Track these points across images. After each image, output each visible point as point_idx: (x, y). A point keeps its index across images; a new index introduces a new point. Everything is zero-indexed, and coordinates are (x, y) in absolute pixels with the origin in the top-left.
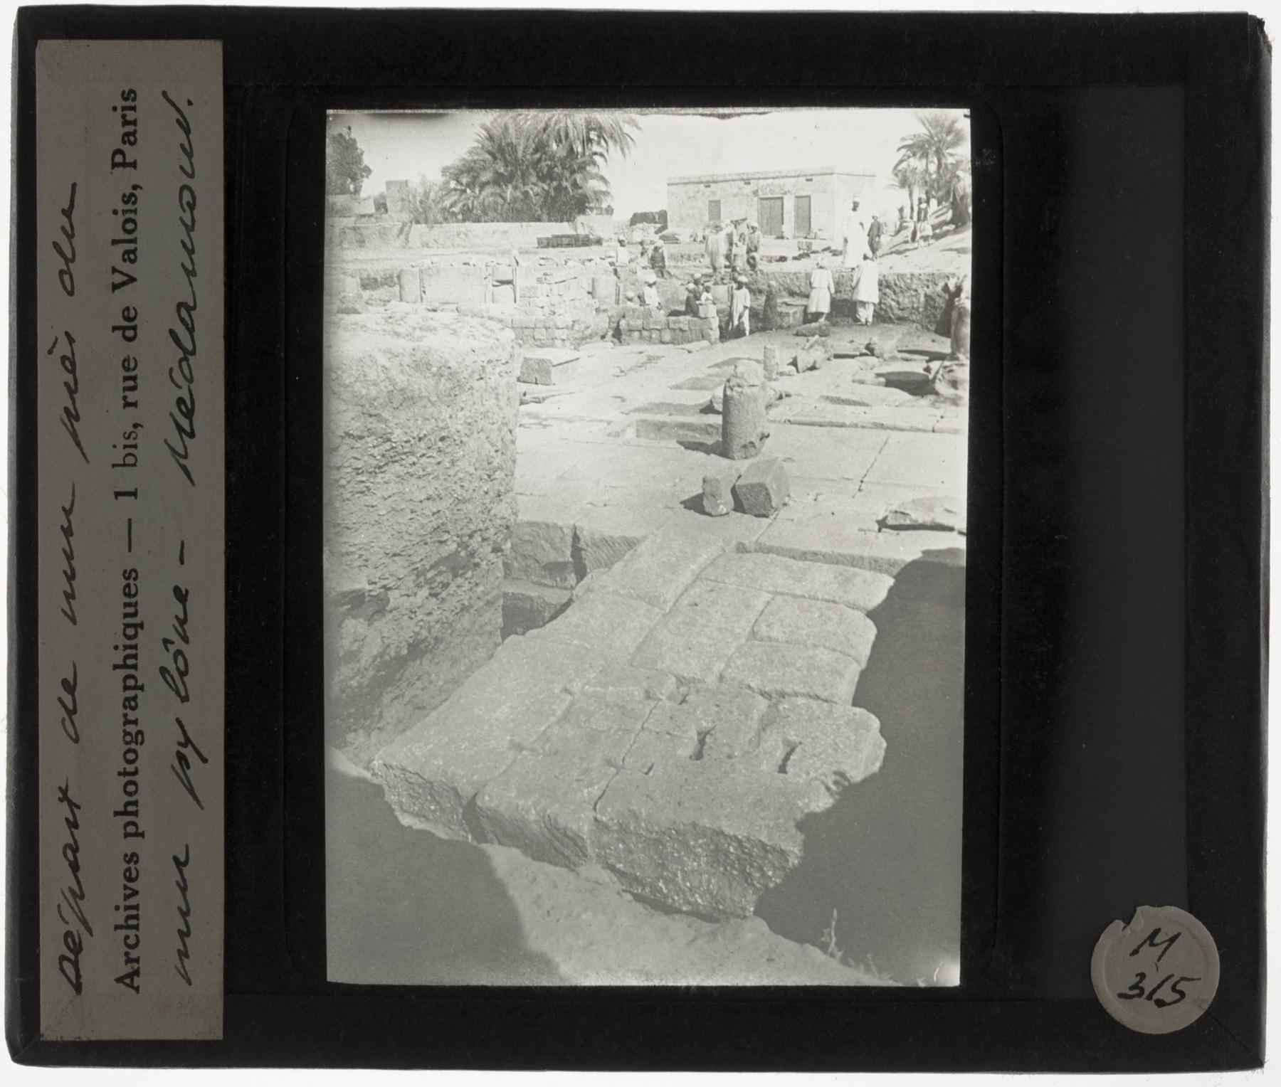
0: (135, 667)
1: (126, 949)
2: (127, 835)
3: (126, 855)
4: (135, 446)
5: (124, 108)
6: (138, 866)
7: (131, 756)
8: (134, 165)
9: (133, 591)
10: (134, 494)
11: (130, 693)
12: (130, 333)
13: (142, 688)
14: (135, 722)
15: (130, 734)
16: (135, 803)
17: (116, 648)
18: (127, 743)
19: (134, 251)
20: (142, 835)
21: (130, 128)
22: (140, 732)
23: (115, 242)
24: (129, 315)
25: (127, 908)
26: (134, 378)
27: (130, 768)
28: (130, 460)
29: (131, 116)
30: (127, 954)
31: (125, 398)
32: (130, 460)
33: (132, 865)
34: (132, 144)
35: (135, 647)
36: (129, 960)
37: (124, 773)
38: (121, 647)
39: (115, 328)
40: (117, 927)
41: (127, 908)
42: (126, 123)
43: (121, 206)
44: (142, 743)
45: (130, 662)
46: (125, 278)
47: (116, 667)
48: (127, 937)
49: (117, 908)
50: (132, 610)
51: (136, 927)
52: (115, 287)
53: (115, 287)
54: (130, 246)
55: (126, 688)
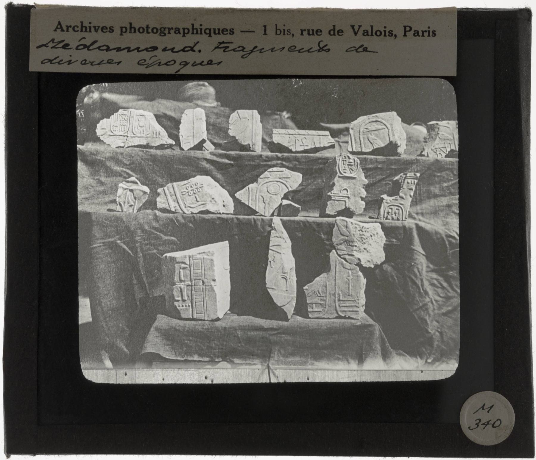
0: (193, 33)
1: (73, 26)
2: (122, 28)
3: (113, 27)
5: (429, 31)
6: (108, 33)
7: (155, 31)
8: (405, 35)
9: (225, 33)
10: (265, 34)
11: (182, 31)
12: (332, 32)
13: (184, 36)
14: (169, 33)
15: (165, 30)
16: (135, 32)
17: (201, 25)
18: (160, 30)
19: (368, 35)
20: (121, 34)
21: (420, 34)
22: (165, 35)
23: (372, 27)
24: (340, 32)
25: (90, 27)
26: (313, 34)
27: (150, 30)
28: (278, 32)
29: (426, 34)
30: (70, 26)
31: (305, 30)
32: (278, 32)
33: (108, 30)
34: (414, 35)
35: (201, 33)
36: (68, 27)
37: (148, 27)
38: (201, 27)
39: (334, 26)
40: (82, 23)
41: (90, 27)
42: (423, 32)
44: (160, 35)
45: (195, 31)
46: (356, 31)
47: (193, 25)
48: (78, 27)
50: (217, 32)
51: (82, 31)
52: (353, 27)
53: (353, 27)
54: (370, 34)
55: (184, 29)
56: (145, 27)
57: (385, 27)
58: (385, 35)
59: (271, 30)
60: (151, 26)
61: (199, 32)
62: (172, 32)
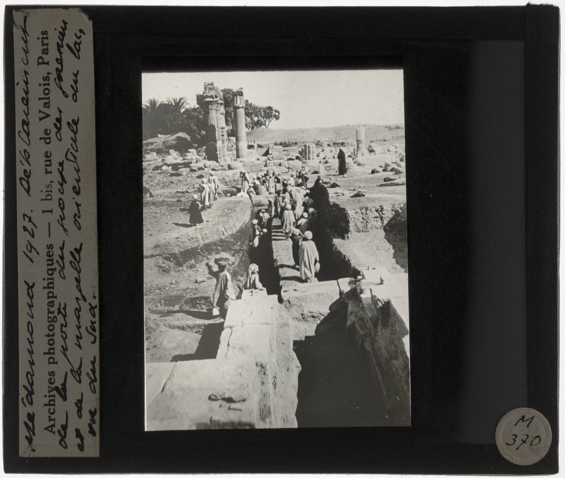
0: (53, 288)
2: (49, 363)
3: (49, 372)
4: (51, 191)
5: (43, 38)
7: (51, 328)
8: (47, 63)
10: (51, 211)
11: (51, 300)
12: (48, 141)
13: (56, 297)
15: (51, 318)
16: (53, 349)
17: (44, 279)
18: (49, 322)
20: (57, 363)
21: (45, 47)
23: (40, 99)
24: (46, 132)
25: (50, 396)
26: (50, 161)
27: (51, 333)
28: (49, 197)
29: (45, 41)
30: (49, 417)
31: (46, 169)
32: (49, 197)
33: (52, 377)
34: (47, 54)
35: (53, 279)
36: (50, 420)
37: (48, 336)
39: (41, 139)
40: (45, 405)
41: (50, 396)
43: (43, 82)
44: (56, 322)
45: (50, 285)
46: (45, 115)
47: (44, 288)
48: (50, 409)
49: (45, 396)
51: (54, 405)
52: (41, 119)
53: (41, 119)
54: (47, 101)
55: (49, 297)
56: (48, 339)
57: (40, 85)
58: (49, 84)
59: (47, 205)
60: (47, 332)
61: (51, 281)
62: (52, 310)
